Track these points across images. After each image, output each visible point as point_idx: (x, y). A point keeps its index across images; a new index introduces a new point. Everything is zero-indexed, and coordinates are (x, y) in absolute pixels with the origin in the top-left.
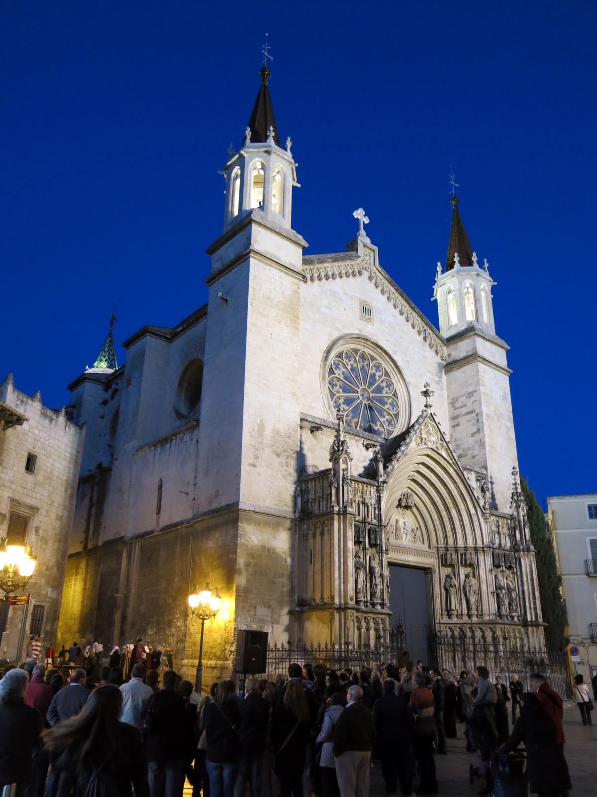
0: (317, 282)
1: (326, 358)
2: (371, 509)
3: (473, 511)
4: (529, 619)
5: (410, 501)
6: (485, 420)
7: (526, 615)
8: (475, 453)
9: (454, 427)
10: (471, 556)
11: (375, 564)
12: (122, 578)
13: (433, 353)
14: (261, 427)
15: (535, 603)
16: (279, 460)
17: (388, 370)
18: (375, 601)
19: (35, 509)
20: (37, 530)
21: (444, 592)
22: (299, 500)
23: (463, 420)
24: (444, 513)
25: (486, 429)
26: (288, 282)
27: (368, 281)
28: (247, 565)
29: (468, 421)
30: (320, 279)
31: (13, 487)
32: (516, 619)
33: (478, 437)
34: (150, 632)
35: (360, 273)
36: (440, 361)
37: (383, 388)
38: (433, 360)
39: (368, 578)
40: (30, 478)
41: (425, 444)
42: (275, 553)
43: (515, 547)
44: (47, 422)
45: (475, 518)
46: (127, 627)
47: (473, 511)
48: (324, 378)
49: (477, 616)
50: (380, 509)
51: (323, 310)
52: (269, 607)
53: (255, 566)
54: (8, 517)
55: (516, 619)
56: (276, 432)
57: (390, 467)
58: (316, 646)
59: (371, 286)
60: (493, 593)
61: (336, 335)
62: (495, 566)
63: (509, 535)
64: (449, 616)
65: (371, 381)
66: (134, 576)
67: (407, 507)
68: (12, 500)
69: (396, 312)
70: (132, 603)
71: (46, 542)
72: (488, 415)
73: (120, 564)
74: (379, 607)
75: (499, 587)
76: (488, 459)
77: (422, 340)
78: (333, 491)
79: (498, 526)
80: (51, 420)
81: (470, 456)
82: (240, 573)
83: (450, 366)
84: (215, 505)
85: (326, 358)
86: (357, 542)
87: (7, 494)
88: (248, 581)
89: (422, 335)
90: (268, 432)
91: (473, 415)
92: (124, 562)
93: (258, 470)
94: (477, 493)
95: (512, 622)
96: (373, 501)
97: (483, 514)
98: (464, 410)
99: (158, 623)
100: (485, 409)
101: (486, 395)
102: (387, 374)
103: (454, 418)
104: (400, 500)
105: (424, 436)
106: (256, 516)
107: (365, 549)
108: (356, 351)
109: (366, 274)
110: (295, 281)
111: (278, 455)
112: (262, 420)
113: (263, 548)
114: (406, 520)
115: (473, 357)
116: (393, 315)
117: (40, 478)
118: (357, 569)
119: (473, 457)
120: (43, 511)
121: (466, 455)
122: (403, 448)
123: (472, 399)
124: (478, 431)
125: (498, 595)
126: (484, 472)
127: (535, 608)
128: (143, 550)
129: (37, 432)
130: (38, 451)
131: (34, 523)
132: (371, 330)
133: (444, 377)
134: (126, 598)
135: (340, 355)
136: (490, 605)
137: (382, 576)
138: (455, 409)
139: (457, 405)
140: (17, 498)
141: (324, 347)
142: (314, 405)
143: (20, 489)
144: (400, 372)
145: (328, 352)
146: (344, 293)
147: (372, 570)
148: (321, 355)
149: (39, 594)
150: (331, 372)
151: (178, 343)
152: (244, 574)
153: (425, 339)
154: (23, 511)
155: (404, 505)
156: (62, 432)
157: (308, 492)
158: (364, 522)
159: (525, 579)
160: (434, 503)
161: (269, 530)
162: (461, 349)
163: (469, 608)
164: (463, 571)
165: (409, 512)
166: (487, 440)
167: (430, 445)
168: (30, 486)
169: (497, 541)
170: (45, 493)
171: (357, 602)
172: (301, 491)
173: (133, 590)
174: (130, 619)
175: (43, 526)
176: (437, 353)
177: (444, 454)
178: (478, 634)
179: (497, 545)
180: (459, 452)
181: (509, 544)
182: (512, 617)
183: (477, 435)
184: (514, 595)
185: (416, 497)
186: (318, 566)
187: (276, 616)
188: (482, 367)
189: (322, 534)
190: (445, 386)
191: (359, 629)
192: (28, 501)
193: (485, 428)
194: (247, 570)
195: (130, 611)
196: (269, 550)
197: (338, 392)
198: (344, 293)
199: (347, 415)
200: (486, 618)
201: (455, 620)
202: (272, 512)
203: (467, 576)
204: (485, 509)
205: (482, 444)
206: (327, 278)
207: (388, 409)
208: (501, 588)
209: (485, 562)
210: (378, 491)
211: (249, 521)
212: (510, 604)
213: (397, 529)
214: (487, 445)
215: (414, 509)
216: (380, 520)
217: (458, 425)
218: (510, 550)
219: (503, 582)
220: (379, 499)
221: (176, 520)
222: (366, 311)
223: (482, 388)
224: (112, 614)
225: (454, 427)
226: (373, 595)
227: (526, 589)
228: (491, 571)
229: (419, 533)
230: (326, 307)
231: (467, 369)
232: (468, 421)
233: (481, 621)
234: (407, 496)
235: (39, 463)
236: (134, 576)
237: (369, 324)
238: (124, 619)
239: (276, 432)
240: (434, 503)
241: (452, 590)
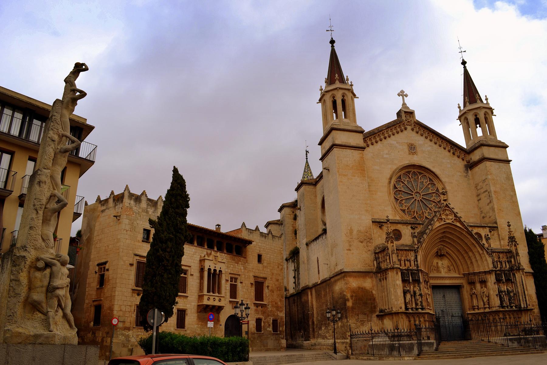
0: (379, 142)
1: (390, 182)
2: (412, 263)
3: (481, 252)
4: (522, 306)
5: (442, 252)
6: (493, 195)
7: (520, 305)
8: (491, 215)
9: (478, 200)
10: (483, 277)
11: (417, 289)
12: (310, 304)
13: (460, 160)
14: (351, 231)
15: (525, 298)
16: (362, 244)
17: (431, 177)
18: (418, 307)
19: (265, 278)
20: (268, 287)
21: (470, 297)
22: (375, 262)
23: (482, 196)
24: (465, 255)
25: (495, 201)
26: (356, 154)
27: (411, 131)
28: (352, 296)
29: (485, 197)
30: (381, 140)
31: (254, 270)
32: (514, 308)
33: (491, 205)
34: (323, 329)
35: (406, 129)
36: (466, 163)
37: (429, 188)
38: (460, 164)
39: (413, 297)
40: (260, 265)
41: (444, 221)
42: (365, 289)
43: (511, 269)
44: (263, 239)
45: (482, 255)
46: (315, 327)
47: (481, 252)
48: (390, 193)
49: (489, 308)
50: (417, 261)
51: (385, 156)
52: (365, 314)
53: (356, 296)
54: (254, 284)
55: (514, 308)
56: (359, 231)
57: (422, 239)
58: (389, 331)
59: (414, 134)
60: (497, 295)
61: (395, 167)
62: (497, 280)
63: (508, 262)
64: (474, 309)
65: (421, 186)
66: (314, 303)
67: (444, 255)
68: (254, 276)
69: (432, 144)
70: (315, 316)
71: (273, 292)
72: (495, 192)
73: (308, 298)
74: (420, 310)
75: (500, 292)
76: (497, 218)
77: (452, 154)
78: (388, 257)
79: (499, 258)
80: (265, 237)
81: (488, 217)
82: (348, 300)
83: (471, 166)
84: (337, 270)
85: (390, 182)
86: (404, 281)
87: (252, 274)
88: (353, 304)
89: (452, 152)
90: (355, 232)
91: (487, 193)
92: (310, 297)
93: (352, 252)
94: (484, 241)
95: (511, 309)
96: (413, 258)
97: (487, 252)
98: (482, 191)
99: (325, 324)
100: (492, 189)
101: (493, 180)
102: (430, 180)
103: (478, 195)
104: (437, 252)
105: (443, 217)
106: (354, 274)
107: (409, 283)
108: (409, 172)
109: (409, 128)
110: (360, 152)
111: (362, 242)
112: (351, 228)
113: (359, 288)
114: (443, 264)
115: (483, 159)
116: (430, 146)
117: (265, 264)
118: (405, 293)
119: (490, 217)
120: (269, 278)
121: (486, 217)
122: (429, 227)
123: (485, 184)
124: (490, 202)
125: (500, 296)
126: (495, 225)
127: (526, 300)
128: (316, 292)
129: (260, 244)
130: (262, 253)
131: (266, 284)
132: (416, 160)
133: (469, 172)
134: (313, 313)
135: (400, 177)
136: (496, 302)
137: (421, 295)
138: (478, 190)
139: (479, 187)
140: (257, 275)
141: (389, 176)
142: (386, 209)
143: (257, 271)
144: (438, 178)
145: (391, 178)
146: (397, 143)
147: (415, 293)
148: (387, 181)
149: (274, 315)
150: (395, 187)
151: (319, 186)
152: (351, 301)
153: (454, 154)
154: (260, 280)
155: (440, 255)
156: (272, 241)
157: (379, 258)
158: (407, 270)
159: (518, 285)
160: (458, 251)
161: (361, 279)
162: (476, 156)
163: (484, 305)
164: (478, 286)
165: (445, 258)
166: (496, 206)
167: (448, 221)
168: (261, 269)
169: (499, 266)
170: (269, 270)
171: (407, 309)
172: (376, 258)
173: (315, 309)
174: (315, 323)
175: (270, 285)
176: (463, 160)
177: (458, 224)
178: (491, 318)
179: (499, 268)
180: (483, 215)
181: (508, 266)
182: (512, 307)
183: (490, 205)
184: (512, 294)
185: (447, 249)
186: (386, 293)
187: (369, 318)
188: (488, 163)
189: (386, 279)
190: (471, 178)
191: (410, 321)
192: (262, 275)
193: (494, 200)
194: (352, 299)
195: (315, 319)
196: (362, 288)
197: (401, 197)
198: (397, 143)
199: (408, 209)
200: (494, 309)
201: (477, 311)
202: (361, 270)
203: (482, 288)
204: (488, 249)
205: (493, 209)
206: (385, 138)
207: (434, 199)
208: (502, 292)
209: (492, 279)
210: (415, 252)
211: (350, 276)
212: (509, 300)
213: (438, 267)
214: (496, 210)
215: (448, 256)
216: (418, 267)
217: (480, 199)
218: (508, 271)
219: (504, 288)
220: (416, 258)
221: (325, 277)
222: (412, 148)
223: (489, 177)
224: (308, 321)
225: (478, 200)
226: (416, 304)
227: (520, 290)
228: (495, 283)
229: (452, 267)
230: (387, 154)
231: (481, 166)
232: (485, 197)
233: (491, 310)
234: (440, 249)
235: (263, 257)
236: (314, 303)
237: (415, 156)
238: (313, 323)
239: (359, 231)
240: (458, 251)
241: (474, 296)
